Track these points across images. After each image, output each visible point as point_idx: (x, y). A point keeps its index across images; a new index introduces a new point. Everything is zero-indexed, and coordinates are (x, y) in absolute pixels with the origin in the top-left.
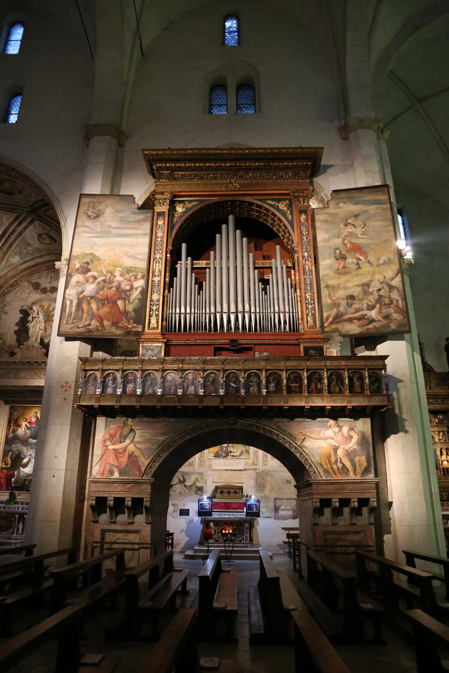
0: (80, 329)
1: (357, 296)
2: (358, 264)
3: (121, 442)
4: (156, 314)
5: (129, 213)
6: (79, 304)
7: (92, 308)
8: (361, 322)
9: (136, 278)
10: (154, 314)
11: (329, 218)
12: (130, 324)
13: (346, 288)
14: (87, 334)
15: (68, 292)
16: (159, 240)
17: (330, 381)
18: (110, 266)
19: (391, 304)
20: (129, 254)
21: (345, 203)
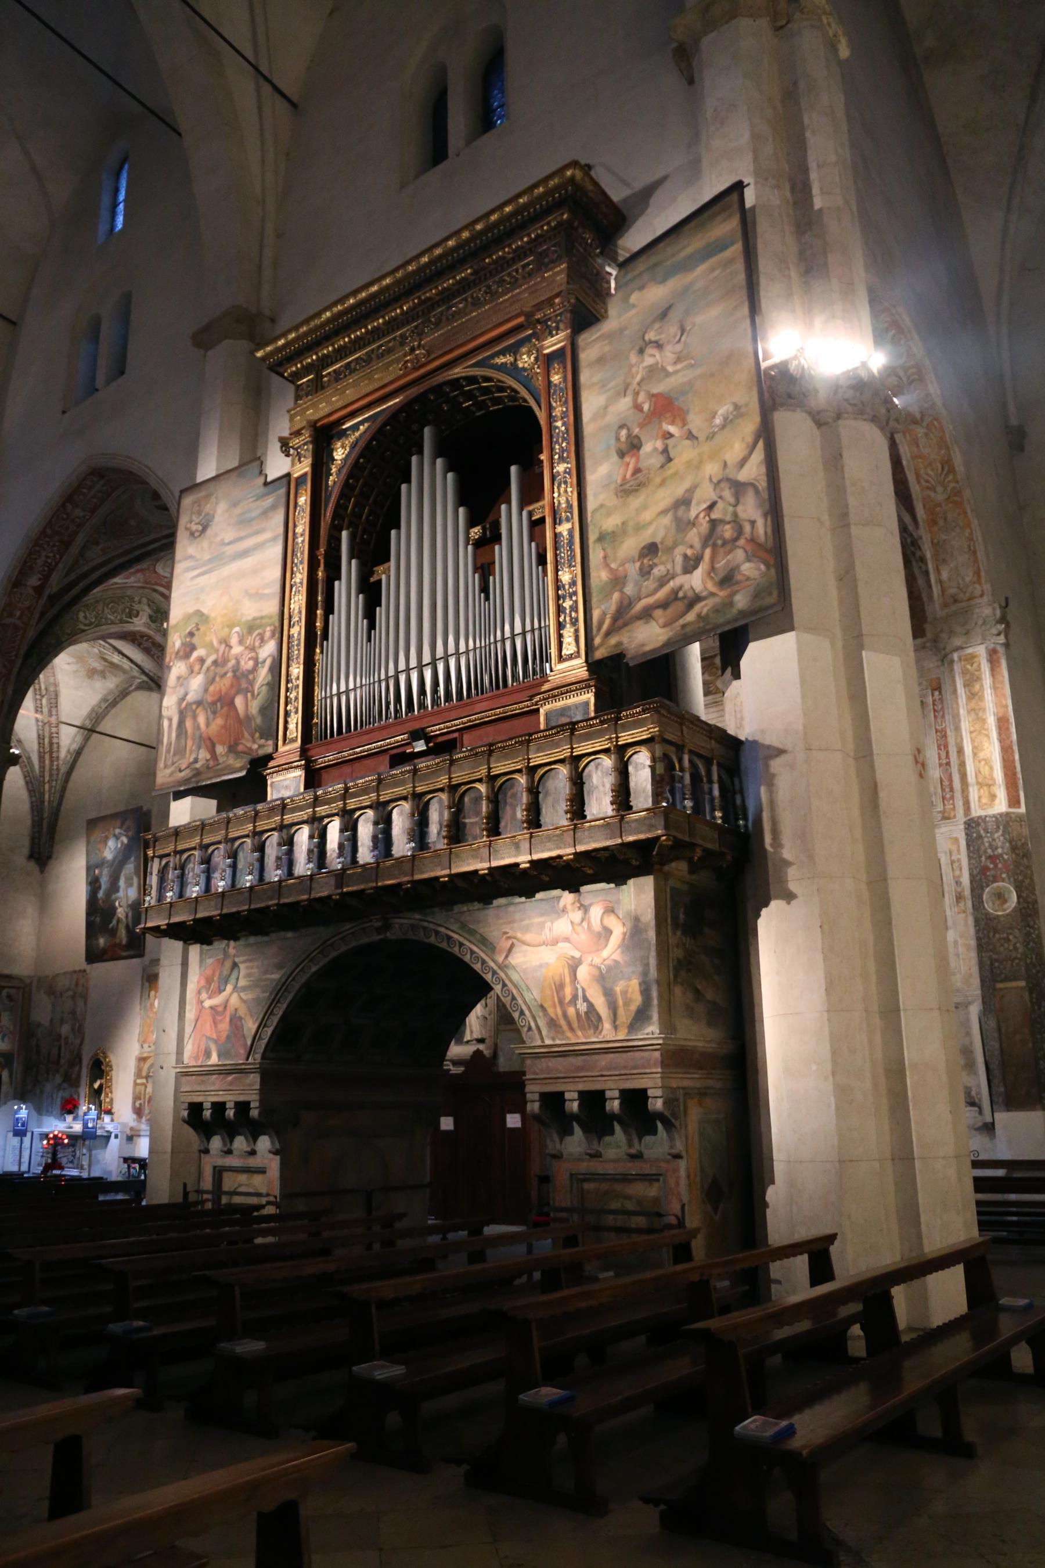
1: (662, 543)
2: (665, 451)
3: (220, 992)
8: (670, 610)
9: (262, 640)
11: (607, 348)
13: (639, 528)
19: (737, 539)
21: (641, 288)
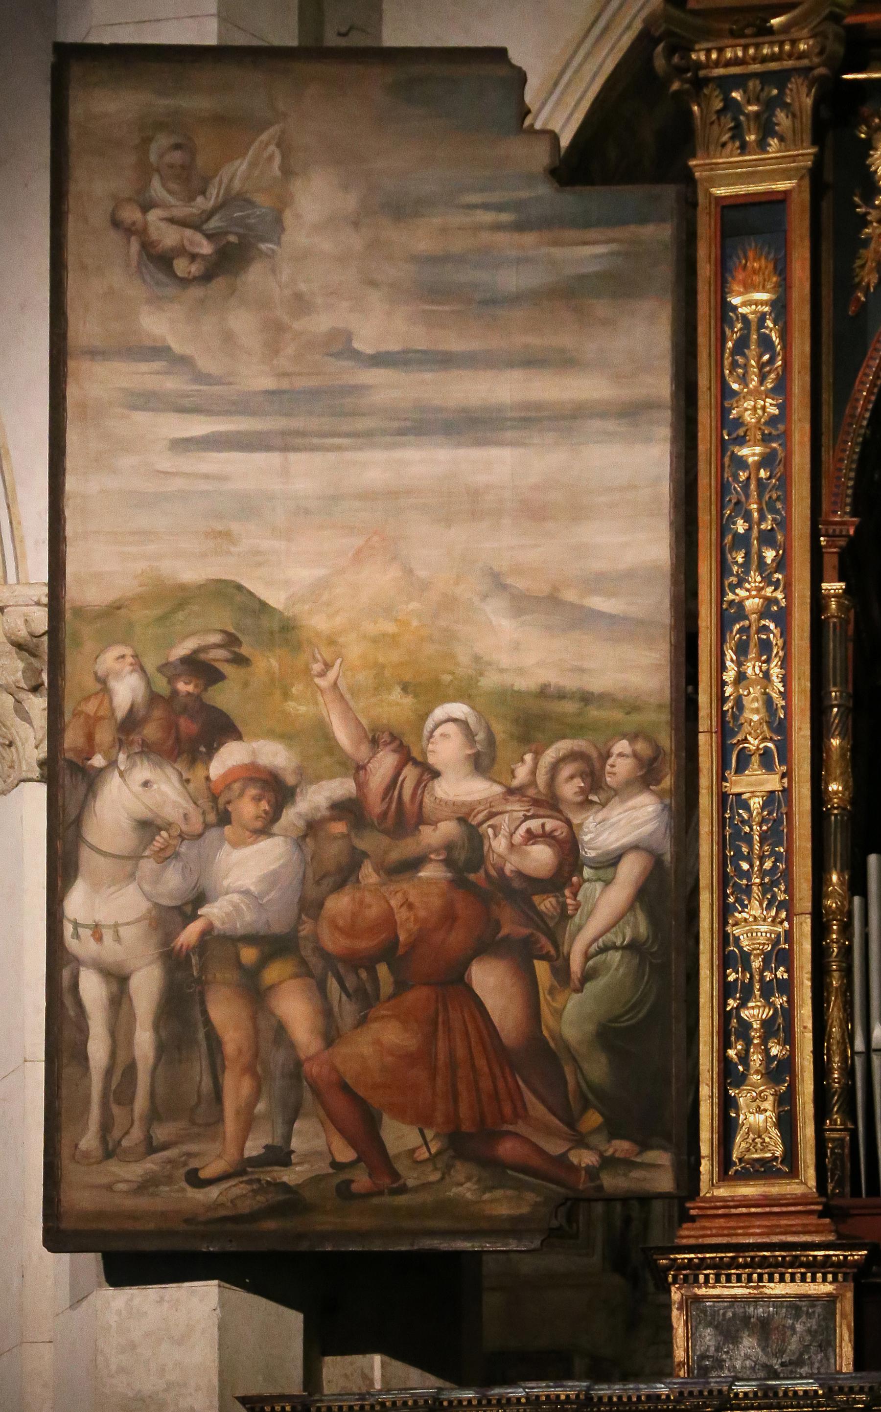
0: (213, 1192)
4: (768, 1058)
5: (488, 217)
6: (181, 1003)
7: (281, 1032)
10: (756, 1059)
12: (581, 1141)
14: (270, 1225)
15: (77, 903)
16: (751, 452)
18: (380, 686)
20: (520, 584)
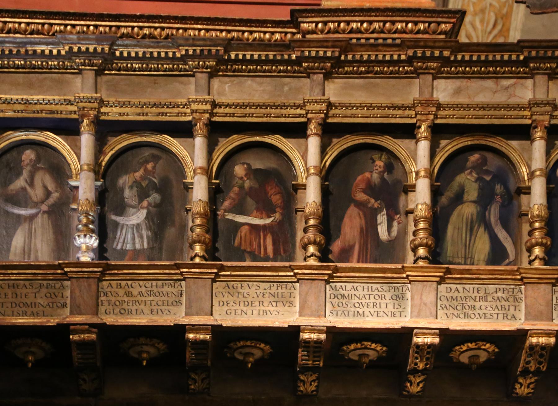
17: (444, 200)
